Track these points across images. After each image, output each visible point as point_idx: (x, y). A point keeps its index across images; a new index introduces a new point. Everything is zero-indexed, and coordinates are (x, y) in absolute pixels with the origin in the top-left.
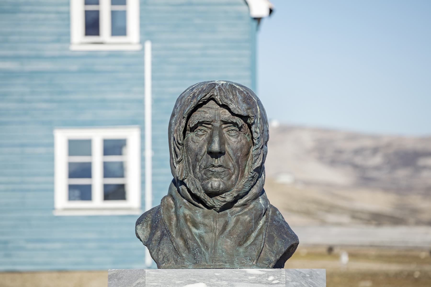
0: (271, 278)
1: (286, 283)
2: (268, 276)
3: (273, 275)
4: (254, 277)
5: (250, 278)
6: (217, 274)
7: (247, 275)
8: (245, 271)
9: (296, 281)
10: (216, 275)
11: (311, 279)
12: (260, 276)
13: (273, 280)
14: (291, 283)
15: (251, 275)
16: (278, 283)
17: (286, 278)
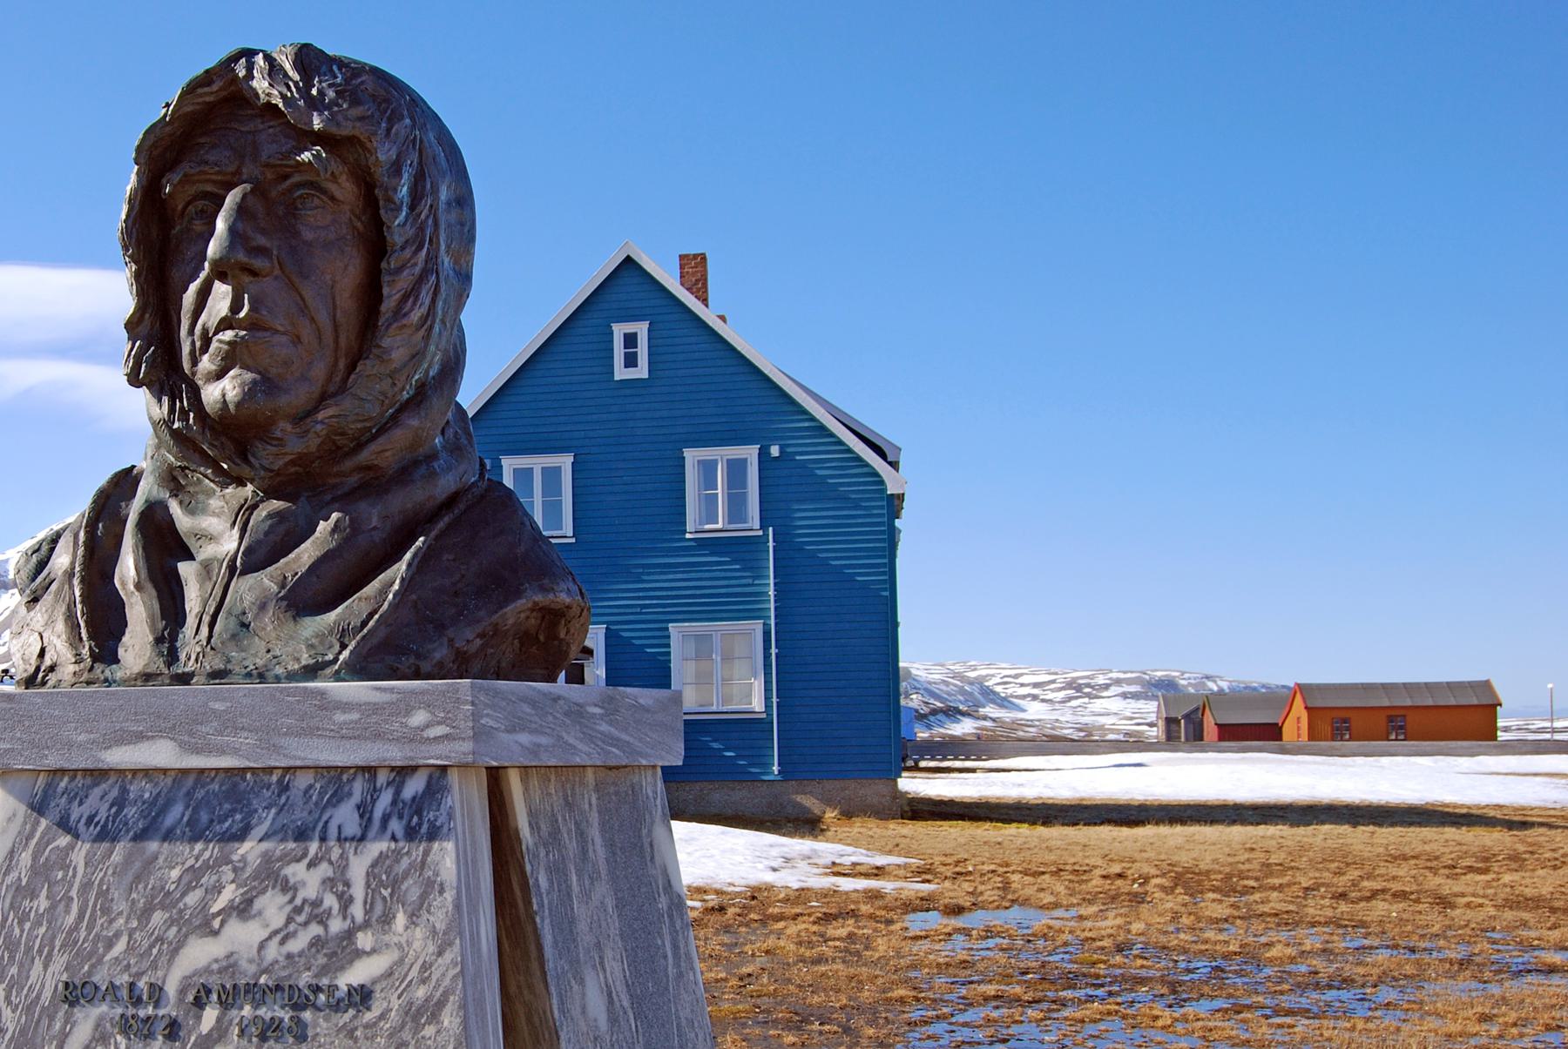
0: (419, 718)
1: (476, 737)
2: (408, 712)
3: (429, 706)
4: (355, 716)
5: (340, 717)
6: (218, 706)
7: (326, 704)
8: (322, 693)
9: (531, 732)
10: (214, 711)
11: (611, 723)
12: (376, 708)
13: (427, 726)
14: (504, 736)
15: (346, 706)
16: (446, 737)
17: (476, 716)
